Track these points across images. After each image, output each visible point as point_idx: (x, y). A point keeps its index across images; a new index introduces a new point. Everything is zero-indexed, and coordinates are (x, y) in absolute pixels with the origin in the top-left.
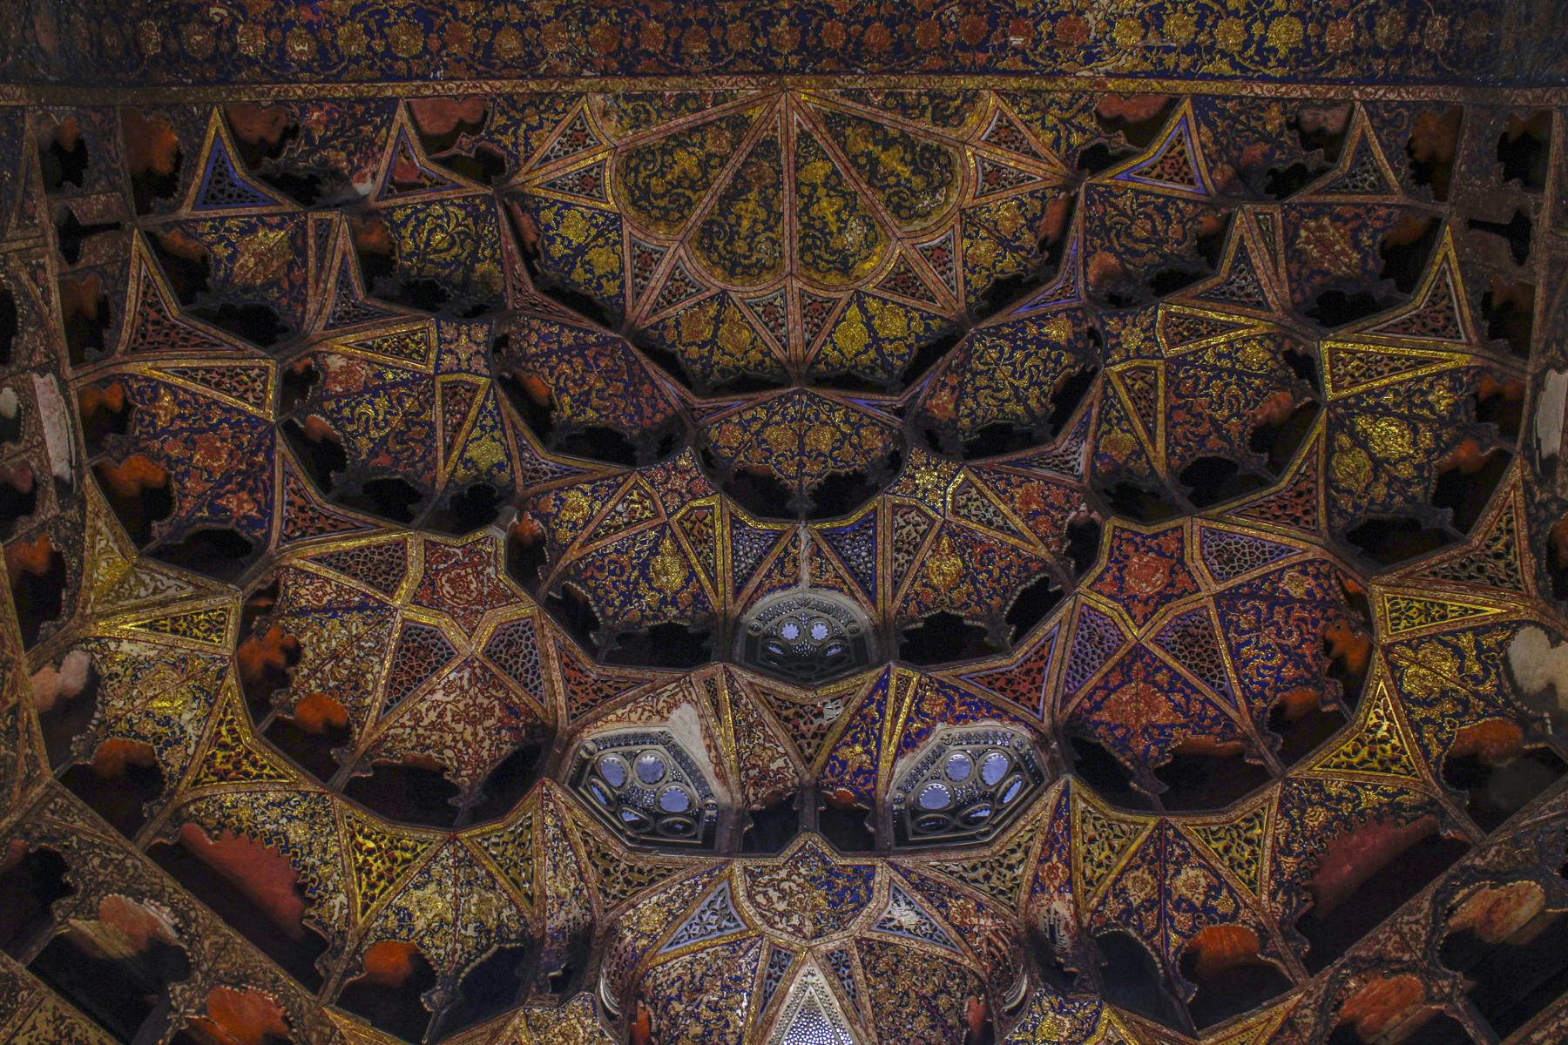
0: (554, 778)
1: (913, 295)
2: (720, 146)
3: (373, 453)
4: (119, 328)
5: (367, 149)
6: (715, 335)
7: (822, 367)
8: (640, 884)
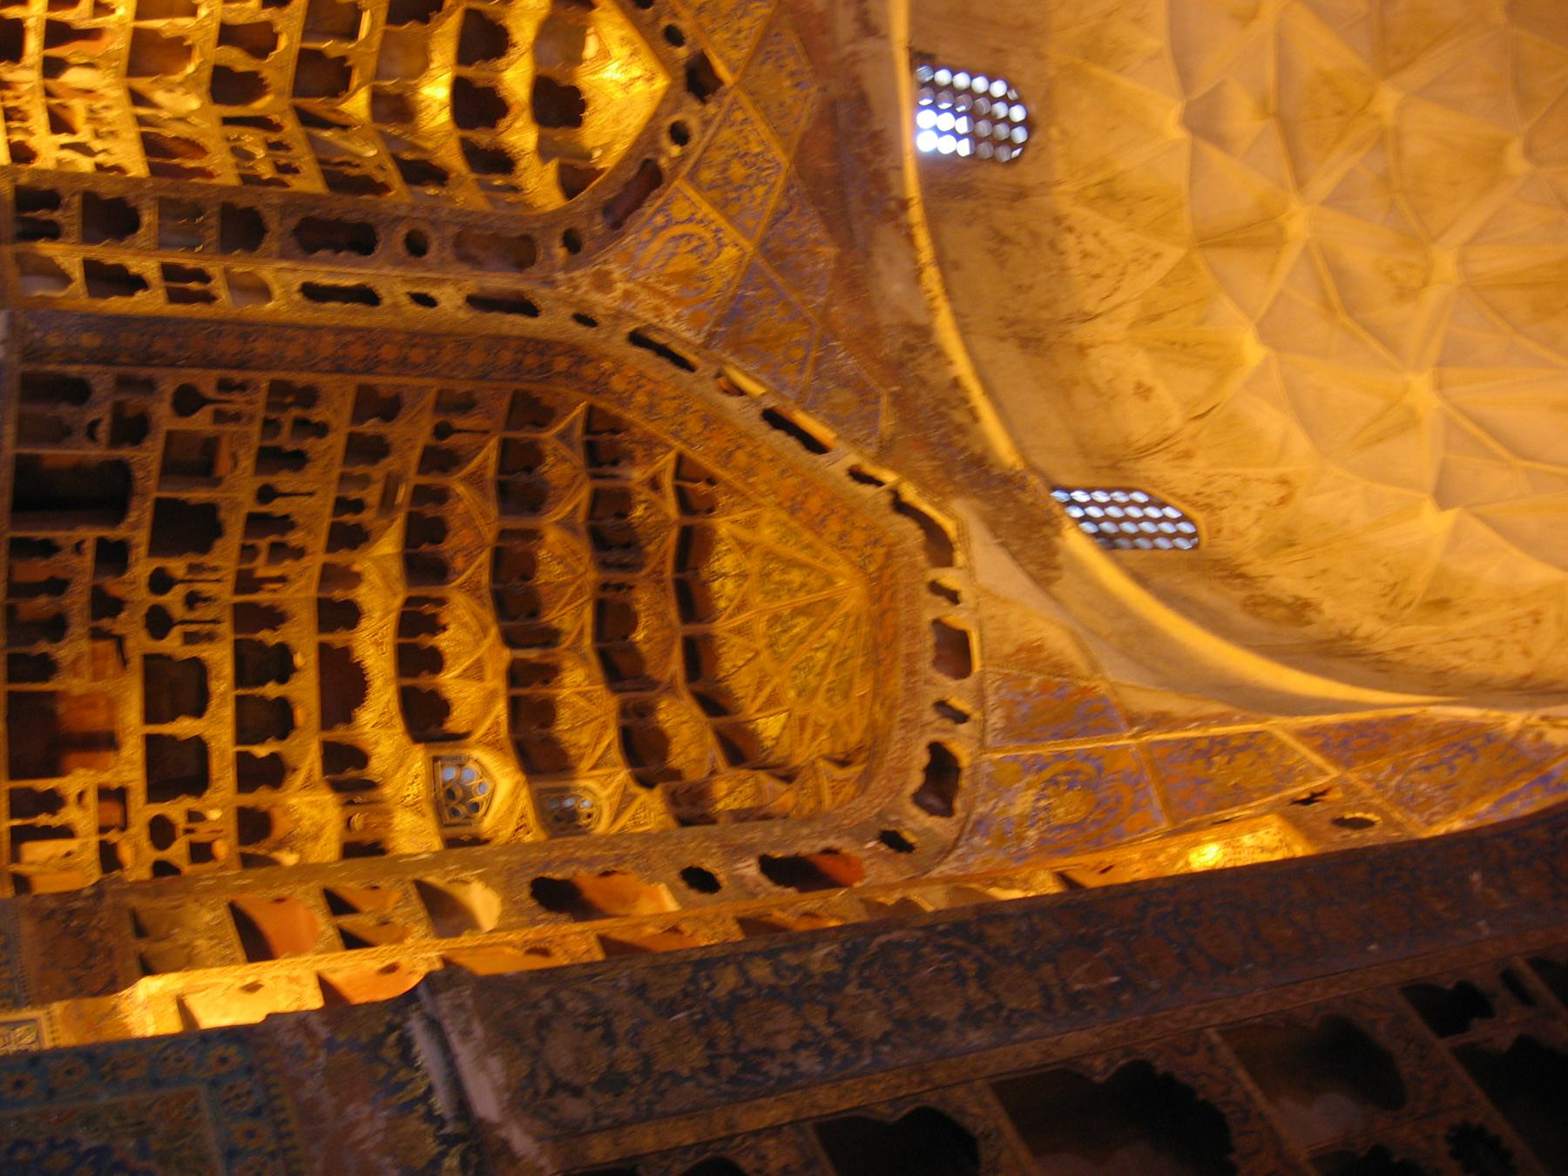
3: (546, 584)
4: (462, 469)
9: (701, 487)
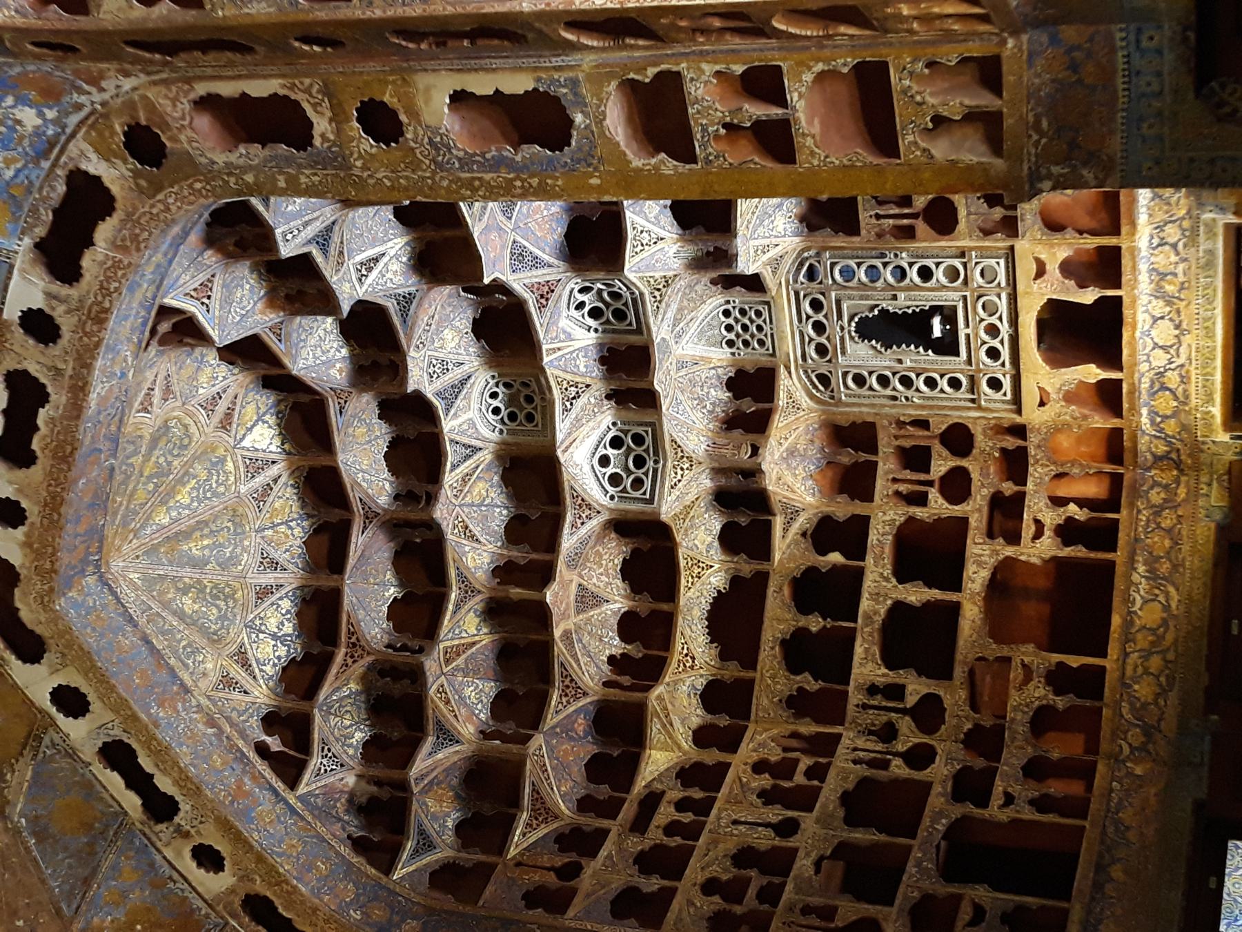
0: (659, 514)
1: (233, 410)
2: (168, 588)
5: (329, 791)
6: (282, 524)
7: (286, 446)
8: (682, 451)
9: (274, 744)
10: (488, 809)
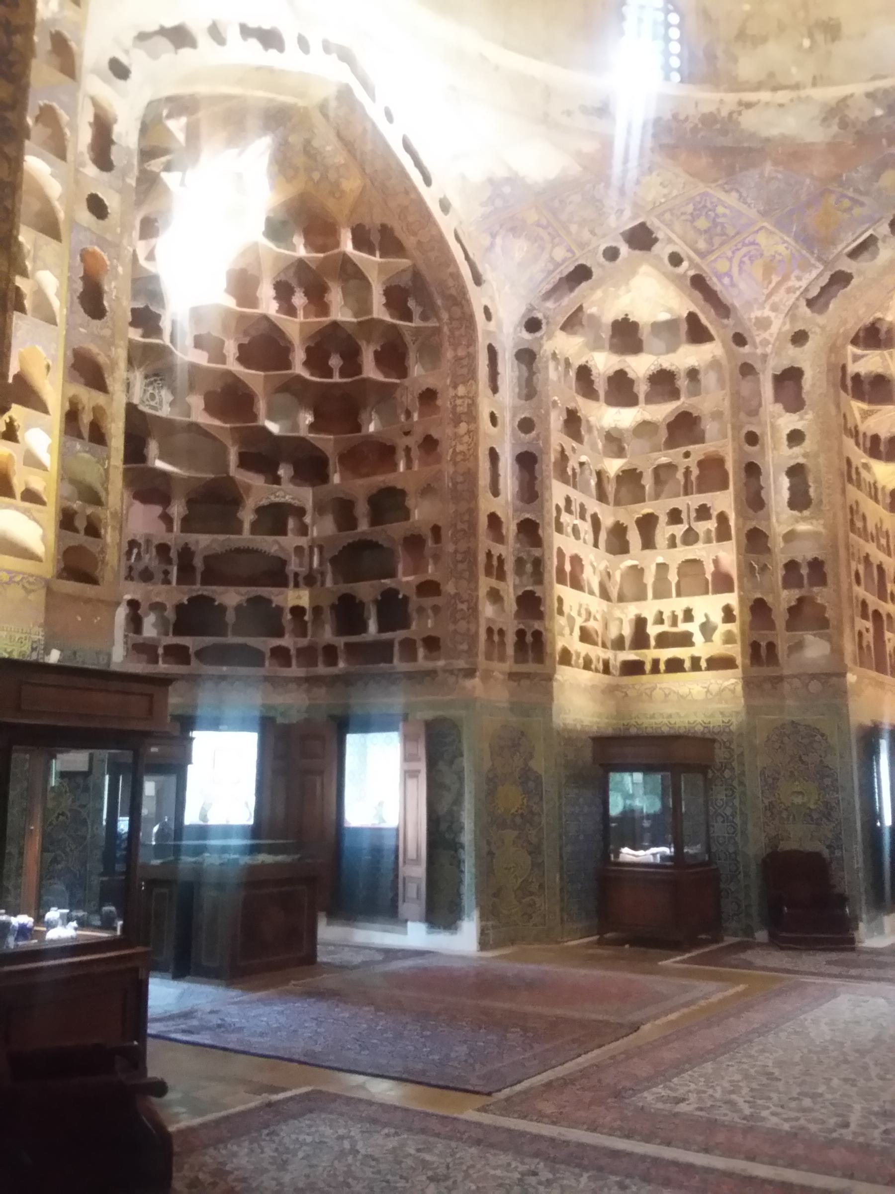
10: (866, 387)
